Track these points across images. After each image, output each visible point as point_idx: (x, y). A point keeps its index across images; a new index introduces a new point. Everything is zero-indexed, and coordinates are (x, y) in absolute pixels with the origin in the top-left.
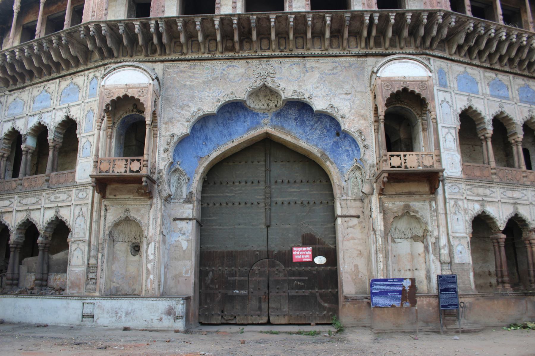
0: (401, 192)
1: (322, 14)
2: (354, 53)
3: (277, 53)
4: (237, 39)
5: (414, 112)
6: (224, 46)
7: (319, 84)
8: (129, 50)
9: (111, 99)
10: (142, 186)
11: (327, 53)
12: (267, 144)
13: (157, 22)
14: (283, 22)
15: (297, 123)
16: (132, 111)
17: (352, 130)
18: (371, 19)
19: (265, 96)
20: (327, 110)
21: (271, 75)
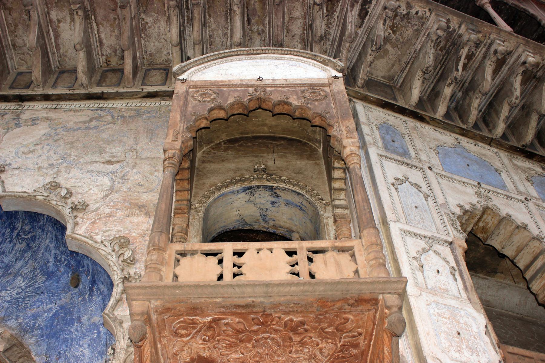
17: (98, 238)
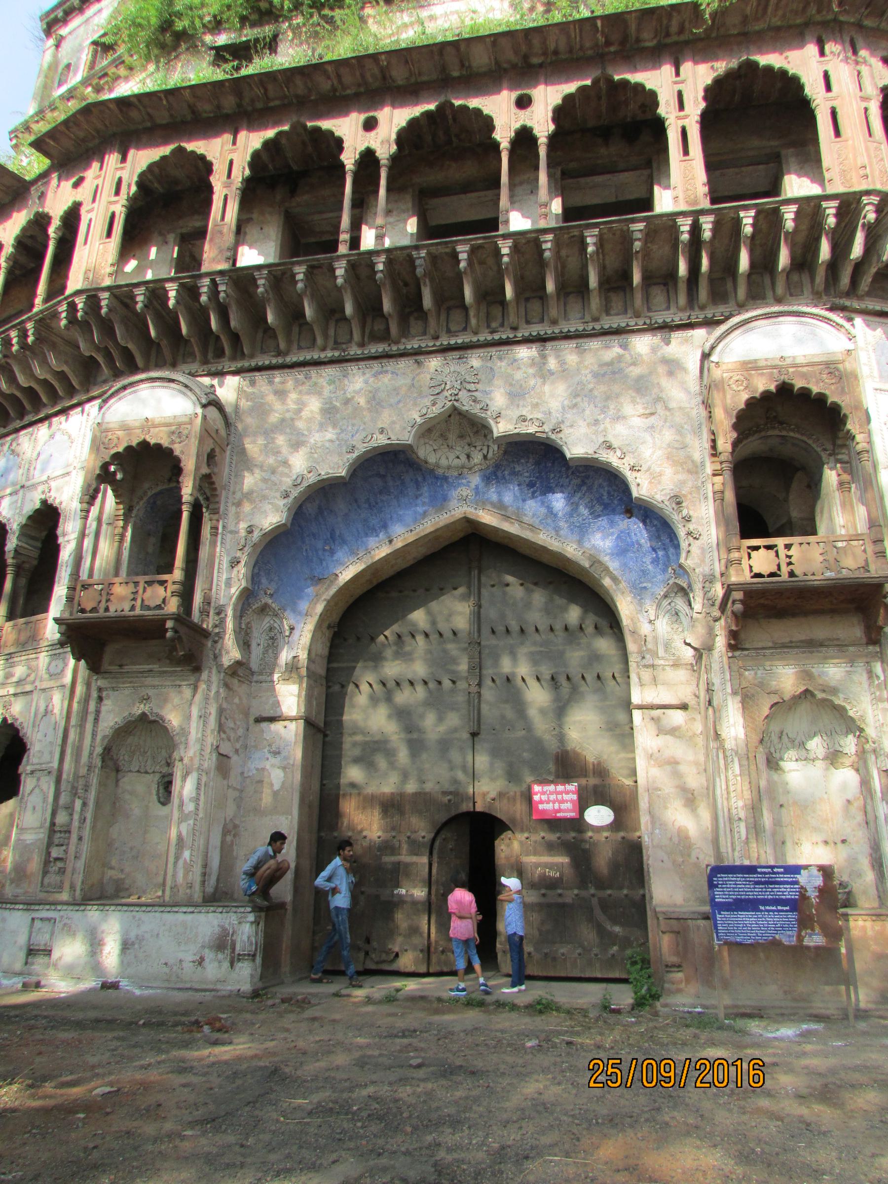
0: (788, 640)
1: (576, 232)
2: (660, 321)
3: (484, 336)
4: (394, 312)
5: (814, 446)
6: (367, 331)
7: (579, 399)
8: (167, 352)
9: (113, 452)
10: (177, 644)
11: (598, 327)
12: (470, 551)
13: (213, 281)
14: (491, 261)
15: (534, 493)
16: (170, 480)
18: (696, 229)
19: (461, 437)
20: (596, 456)
21: (469, 387)
